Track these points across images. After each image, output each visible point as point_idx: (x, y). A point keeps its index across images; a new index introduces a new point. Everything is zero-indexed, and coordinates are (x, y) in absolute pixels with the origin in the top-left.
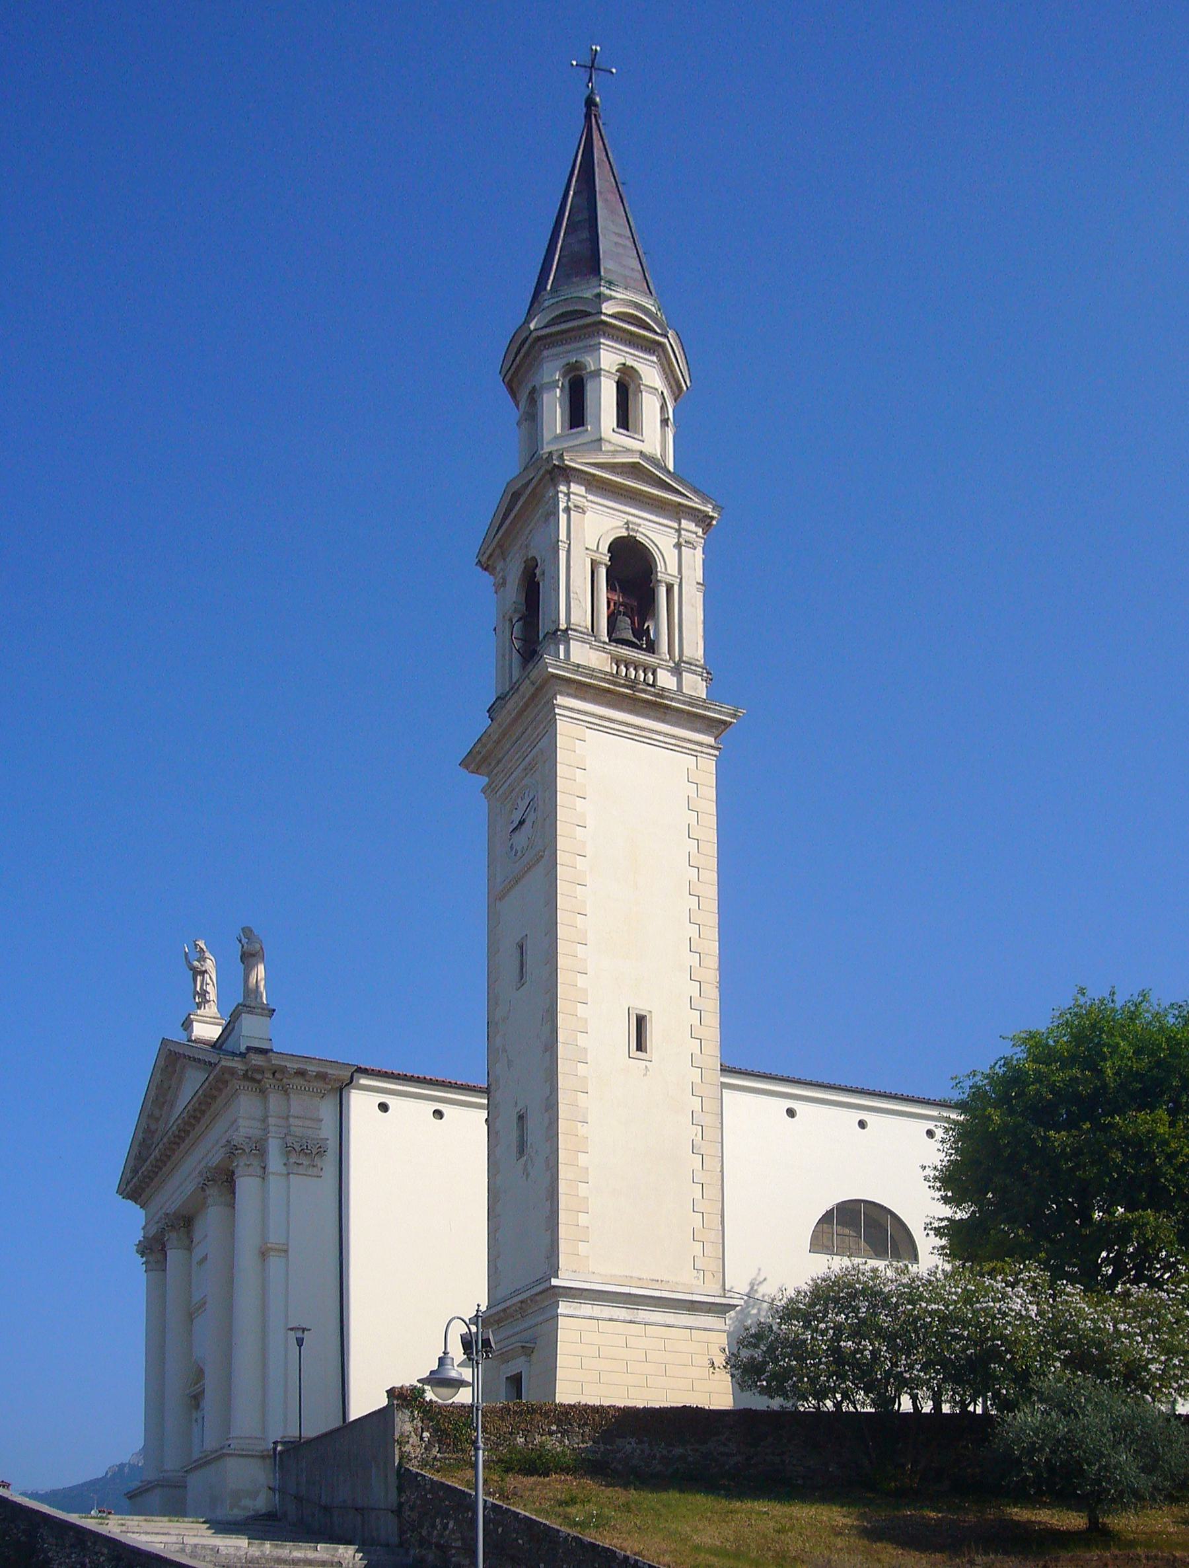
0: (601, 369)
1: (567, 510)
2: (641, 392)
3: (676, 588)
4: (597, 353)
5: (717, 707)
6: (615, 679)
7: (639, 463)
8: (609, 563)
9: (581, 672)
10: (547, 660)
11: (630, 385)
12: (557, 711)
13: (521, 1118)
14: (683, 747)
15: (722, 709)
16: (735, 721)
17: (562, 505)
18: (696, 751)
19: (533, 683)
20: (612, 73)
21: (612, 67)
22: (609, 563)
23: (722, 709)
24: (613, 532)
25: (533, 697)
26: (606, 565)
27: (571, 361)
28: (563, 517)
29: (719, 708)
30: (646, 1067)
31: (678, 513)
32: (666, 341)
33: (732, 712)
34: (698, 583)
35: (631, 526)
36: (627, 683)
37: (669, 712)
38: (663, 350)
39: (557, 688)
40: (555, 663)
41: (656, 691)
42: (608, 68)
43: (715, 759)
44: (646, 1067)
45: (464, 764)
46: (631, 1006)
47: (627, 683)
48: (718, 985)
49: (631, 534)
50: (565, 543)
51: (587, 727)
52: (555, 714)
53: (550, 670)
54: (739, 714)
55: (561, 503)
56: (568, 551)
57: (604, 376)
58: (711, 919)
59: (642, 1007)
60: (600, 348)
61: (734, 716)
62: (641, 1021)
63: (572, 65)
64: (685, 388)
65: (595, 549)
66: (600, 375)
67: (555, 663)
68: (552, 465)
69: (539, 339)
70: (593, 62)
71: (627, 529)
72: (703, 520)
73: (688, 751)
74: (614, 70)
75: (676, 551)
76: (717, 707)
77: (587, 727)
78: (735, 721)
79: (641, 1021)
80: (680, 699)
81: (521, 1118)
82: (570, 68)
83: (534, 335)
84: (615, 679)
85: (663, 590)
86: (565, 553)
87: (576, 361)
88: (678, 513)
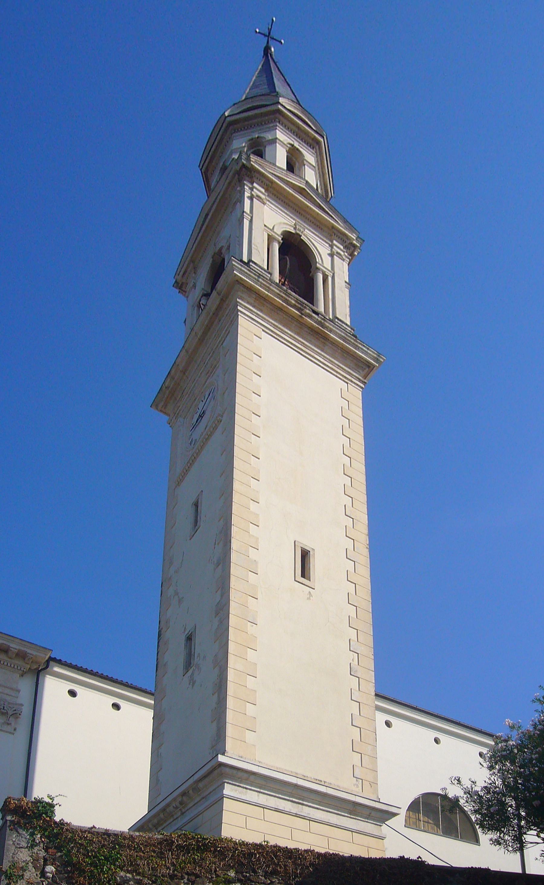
0: (276, 138)
1: (251, 198)
2: (304, 165)
3: (330, 279)
4: (274, 131)
5: (364, 348)
6: (287, 298)
7: (304, 189)
8: (282, 241)
9: (261, 283)
10: (234, 263)
11: (295, 164)
12: (239, 308)
13: (189, 639)
14: (337, 372)
15: (369, 351)
16: (377, 365)
17: (247, 194)
18: (348, 379)
19: (219, 294)
20: (282, 43)
21: (281, 39)
22: (282, 241)
23: (369, 351)
24: (285, 226)
25: (219, 308)
26: (279, 242)
27: (254, 137)
28: (247, 202)
29: (366, 350)
30: (309, 592)
31: (331, 235)
32: (322, 140)
33: (375, 356)
34: (346, 282)
35: (298, 227)
36: (297, 304)
37: (328, 343)
38: (319, 148)
39: (239, 293)
40: (240, 267)
41: (319, 319)
42: (279, 40)
43: (361, 390)
44: (309, 592)
45: (155, 404)
46: (297, 540)
47: (297, 304)
48: (368, 547)
49: (298, 232)
50: (248, 215)
51: (263, 330)
52: (238, 311)
53: (235, 272)
54: (381, 360)
55: (246, 193)
56: (251, 221)
57: (279, 144)
58: (361, 497)
59: (308, 545)
60: (276, 129)
61: (377, 360)
62: (305, 555)
63: (256, 31)
64: (330, 196)
65: (271, 228)
66: (276, 142)
67: (240, 267)
68: (241, 164)
69: (231, 124)
70: (269, 33)
71: (295, 229)
72: (350, 247)
73: (341, 377)
74: (283, 41)
75: (330, 258)
76: (364, 348)
77: (263, 330)
78: (377, 365)
79: (305, 555)
80: (336, 332)
81: (189, 639)
82: (254, 33)
83: (228, 119)
84: (287, 298)
85: (320, 277)
86: (248, 222)
87: (258, 137)
88: (331, 235)
